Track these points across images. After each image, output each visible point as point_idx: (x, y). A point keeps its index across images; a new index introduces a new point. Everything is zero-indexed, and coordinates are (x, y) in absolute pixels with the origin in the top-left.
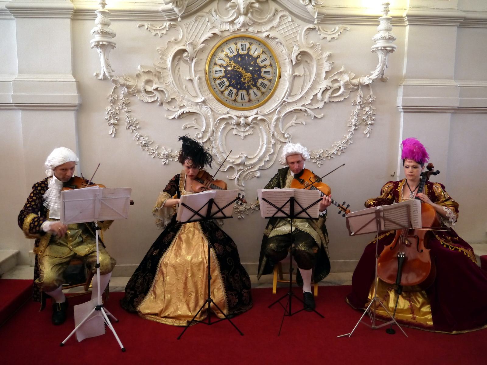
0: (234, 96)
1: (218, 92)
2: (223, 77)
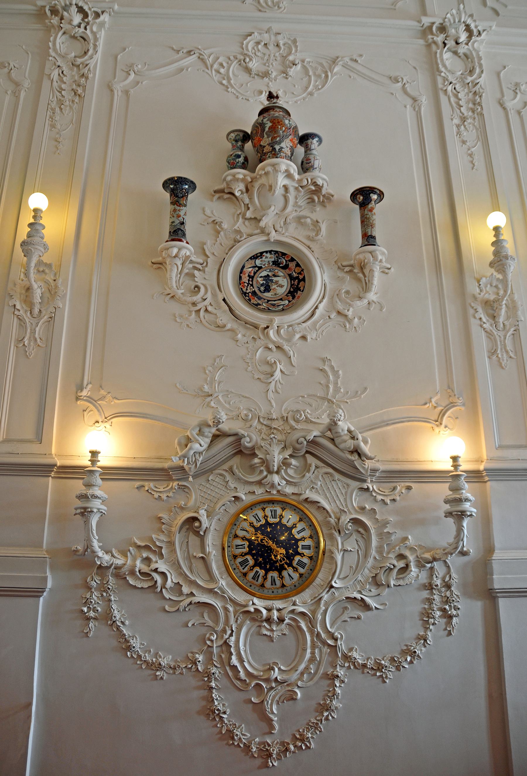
0: (260, 580)
1: (240, 574)
2: (246, 554)
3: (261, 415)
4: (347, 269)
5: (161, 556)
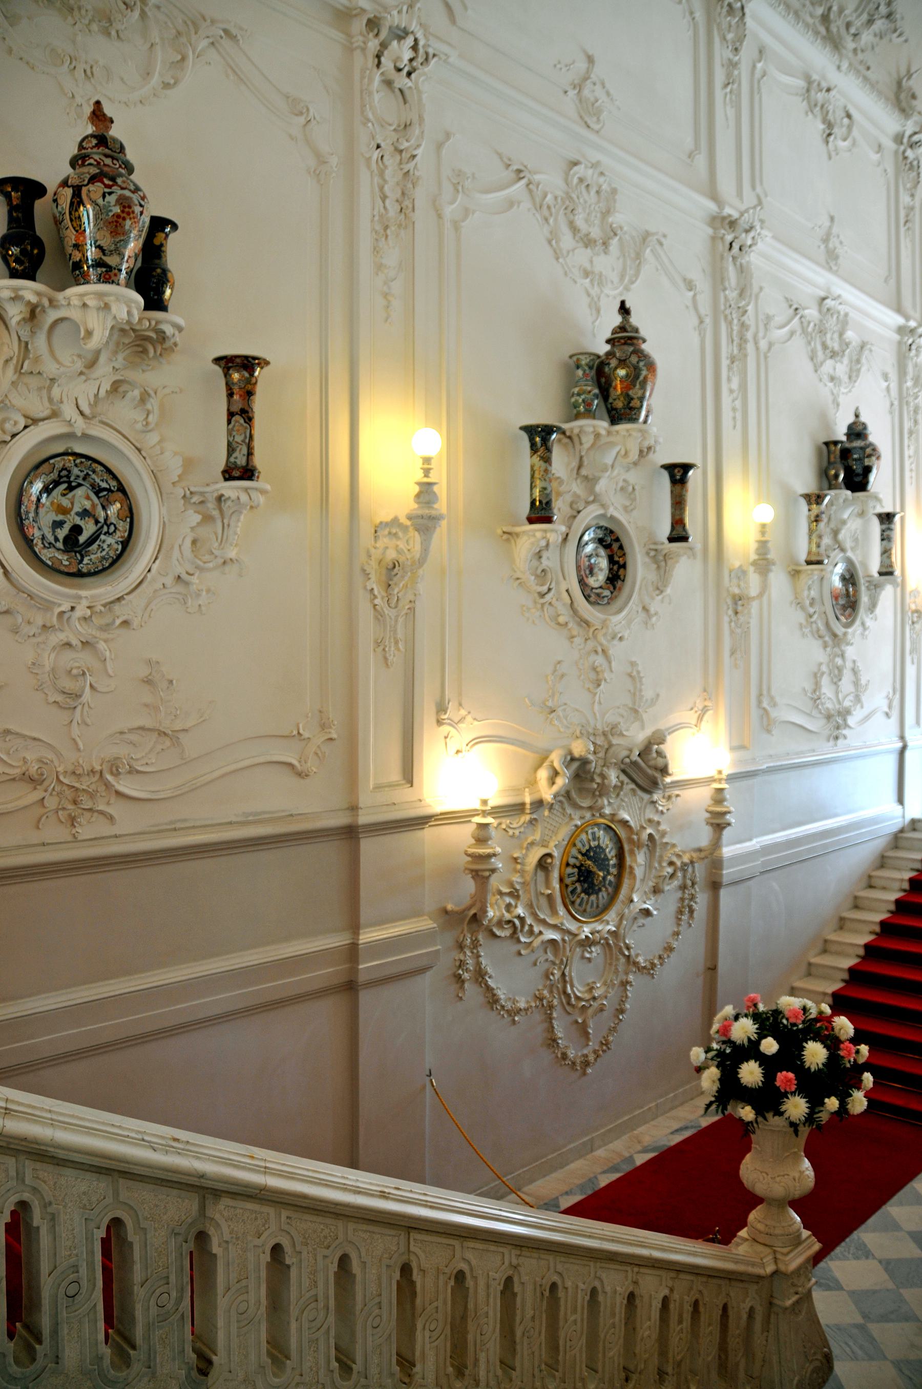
3: (591, 730)
4: (652, 553)
5: (517, 897)
